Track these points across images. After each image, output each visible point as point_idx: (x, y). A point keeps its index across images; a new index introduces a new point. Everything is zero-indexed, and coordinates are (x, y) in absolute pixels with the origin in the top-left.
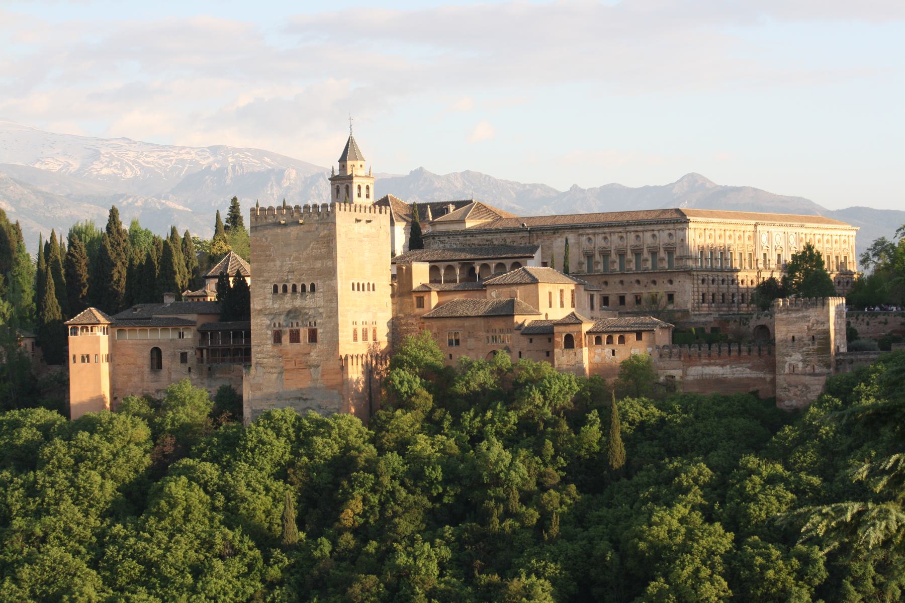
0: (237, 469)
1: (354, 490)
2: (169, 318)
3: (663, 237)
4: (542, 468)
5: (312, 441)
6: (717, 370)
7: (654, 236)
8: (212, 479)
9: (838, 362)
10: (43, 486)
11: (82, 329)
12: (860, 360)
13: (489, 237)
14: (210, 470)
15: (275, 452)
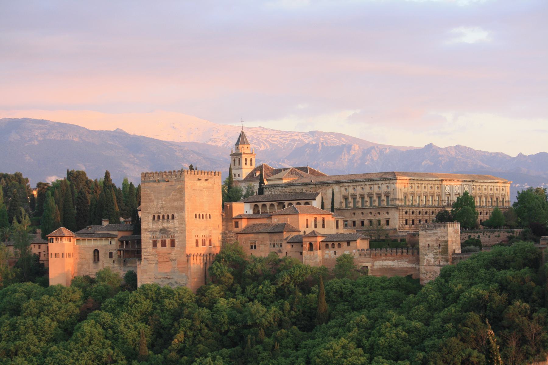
0: (121, 316)
1: (180, 328)
2: (103, 233)
3: (384, 188)
6: (390, 263)
7: (379, 187)
8: (107, 321)
9: (454, 259)
10: (20, 324)
11: (56, 239)
12: (465, 257)
13: (294, 188)
14: (107, 317)
15: (143, 307)
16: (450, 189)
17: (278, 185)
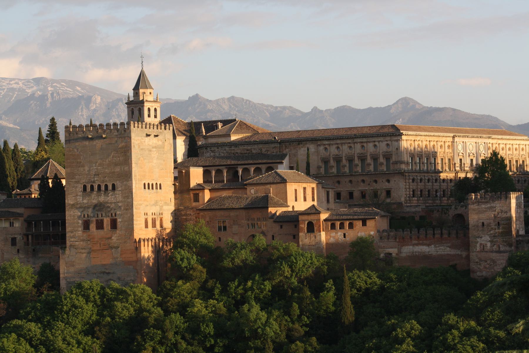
0: (55, 327)
1: (146, 343)
3: (382, 147)
4: (291, 325)
5: (114, 305)
6: (424, 249)
8: (36, 335)
14: (34, 328)
15: (85, 314)
16: (463, 148)
17: (225, 143)
